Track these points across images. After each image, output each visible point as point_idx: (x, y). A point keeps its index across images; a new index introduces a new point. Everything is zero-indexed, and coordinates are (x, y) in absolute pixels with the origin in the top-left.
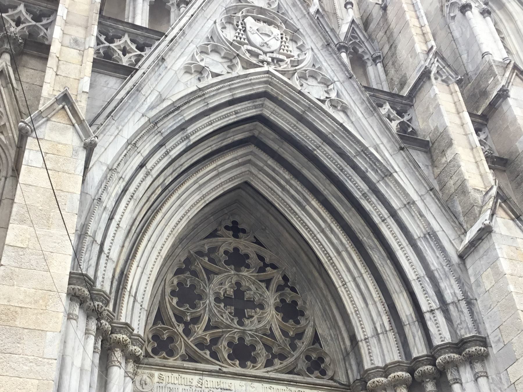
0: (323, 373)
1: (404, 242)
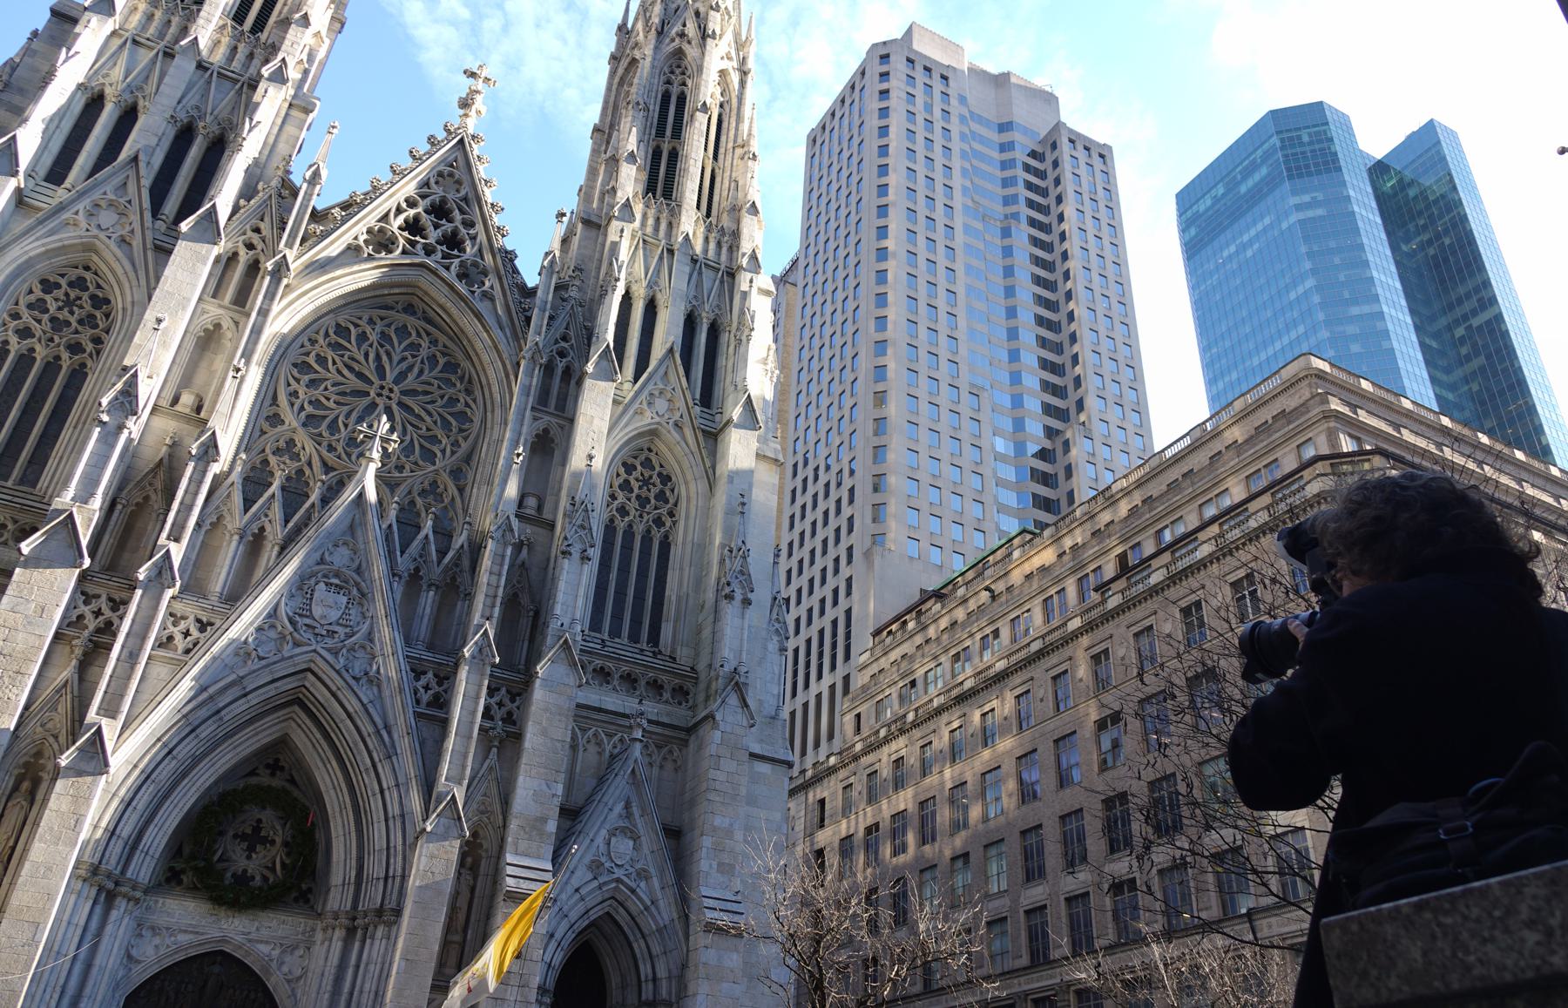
0: (307, 901)
1: (382, 818)
